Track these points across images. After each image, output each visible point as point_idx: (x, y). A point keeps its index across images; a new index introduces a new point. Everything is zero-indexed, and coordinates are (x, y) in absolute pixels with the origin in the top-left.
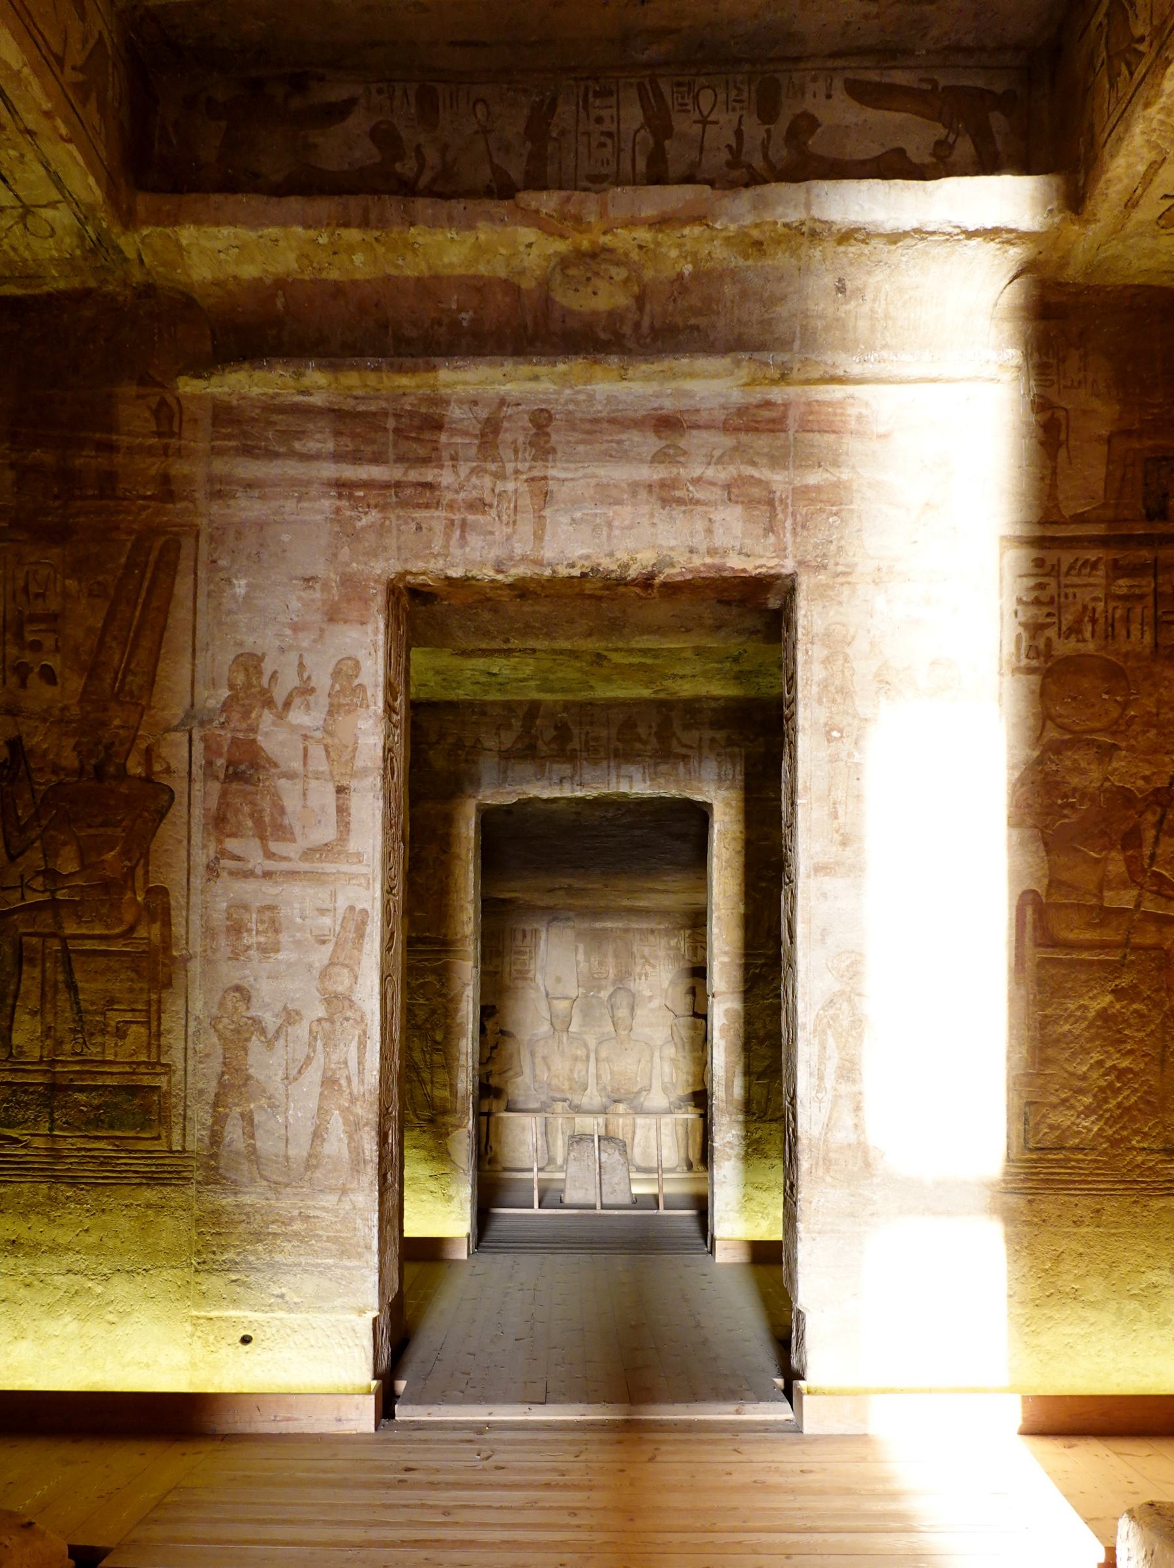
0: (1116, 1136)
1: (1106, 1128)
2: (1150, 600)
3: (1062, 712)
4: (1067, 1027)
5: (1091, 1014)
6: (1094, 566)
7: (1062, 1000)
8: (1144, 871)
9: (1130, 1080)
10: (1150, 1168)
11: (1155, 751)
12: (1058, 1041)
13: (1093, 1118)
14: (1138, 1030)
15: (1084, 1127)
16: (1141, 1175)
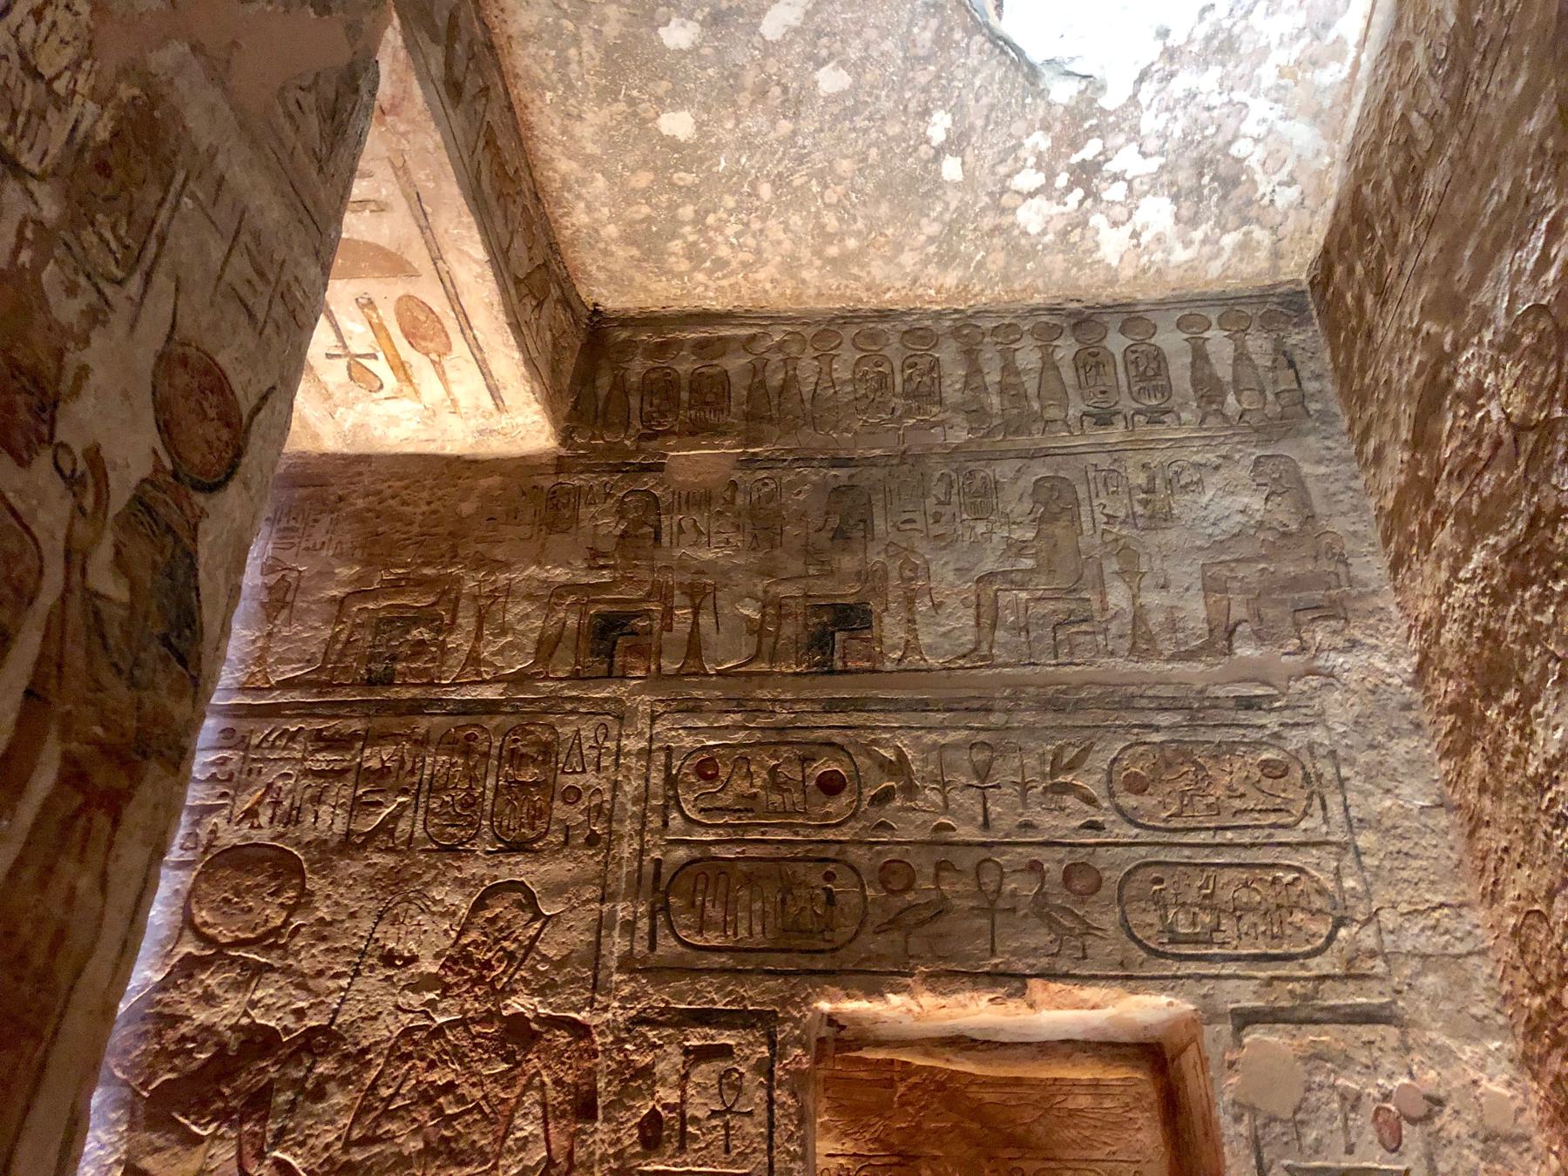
2: (351, 776)
3: (210, 920)
6: (293, 737)
8: (260, 1155)
11: (320, 973)
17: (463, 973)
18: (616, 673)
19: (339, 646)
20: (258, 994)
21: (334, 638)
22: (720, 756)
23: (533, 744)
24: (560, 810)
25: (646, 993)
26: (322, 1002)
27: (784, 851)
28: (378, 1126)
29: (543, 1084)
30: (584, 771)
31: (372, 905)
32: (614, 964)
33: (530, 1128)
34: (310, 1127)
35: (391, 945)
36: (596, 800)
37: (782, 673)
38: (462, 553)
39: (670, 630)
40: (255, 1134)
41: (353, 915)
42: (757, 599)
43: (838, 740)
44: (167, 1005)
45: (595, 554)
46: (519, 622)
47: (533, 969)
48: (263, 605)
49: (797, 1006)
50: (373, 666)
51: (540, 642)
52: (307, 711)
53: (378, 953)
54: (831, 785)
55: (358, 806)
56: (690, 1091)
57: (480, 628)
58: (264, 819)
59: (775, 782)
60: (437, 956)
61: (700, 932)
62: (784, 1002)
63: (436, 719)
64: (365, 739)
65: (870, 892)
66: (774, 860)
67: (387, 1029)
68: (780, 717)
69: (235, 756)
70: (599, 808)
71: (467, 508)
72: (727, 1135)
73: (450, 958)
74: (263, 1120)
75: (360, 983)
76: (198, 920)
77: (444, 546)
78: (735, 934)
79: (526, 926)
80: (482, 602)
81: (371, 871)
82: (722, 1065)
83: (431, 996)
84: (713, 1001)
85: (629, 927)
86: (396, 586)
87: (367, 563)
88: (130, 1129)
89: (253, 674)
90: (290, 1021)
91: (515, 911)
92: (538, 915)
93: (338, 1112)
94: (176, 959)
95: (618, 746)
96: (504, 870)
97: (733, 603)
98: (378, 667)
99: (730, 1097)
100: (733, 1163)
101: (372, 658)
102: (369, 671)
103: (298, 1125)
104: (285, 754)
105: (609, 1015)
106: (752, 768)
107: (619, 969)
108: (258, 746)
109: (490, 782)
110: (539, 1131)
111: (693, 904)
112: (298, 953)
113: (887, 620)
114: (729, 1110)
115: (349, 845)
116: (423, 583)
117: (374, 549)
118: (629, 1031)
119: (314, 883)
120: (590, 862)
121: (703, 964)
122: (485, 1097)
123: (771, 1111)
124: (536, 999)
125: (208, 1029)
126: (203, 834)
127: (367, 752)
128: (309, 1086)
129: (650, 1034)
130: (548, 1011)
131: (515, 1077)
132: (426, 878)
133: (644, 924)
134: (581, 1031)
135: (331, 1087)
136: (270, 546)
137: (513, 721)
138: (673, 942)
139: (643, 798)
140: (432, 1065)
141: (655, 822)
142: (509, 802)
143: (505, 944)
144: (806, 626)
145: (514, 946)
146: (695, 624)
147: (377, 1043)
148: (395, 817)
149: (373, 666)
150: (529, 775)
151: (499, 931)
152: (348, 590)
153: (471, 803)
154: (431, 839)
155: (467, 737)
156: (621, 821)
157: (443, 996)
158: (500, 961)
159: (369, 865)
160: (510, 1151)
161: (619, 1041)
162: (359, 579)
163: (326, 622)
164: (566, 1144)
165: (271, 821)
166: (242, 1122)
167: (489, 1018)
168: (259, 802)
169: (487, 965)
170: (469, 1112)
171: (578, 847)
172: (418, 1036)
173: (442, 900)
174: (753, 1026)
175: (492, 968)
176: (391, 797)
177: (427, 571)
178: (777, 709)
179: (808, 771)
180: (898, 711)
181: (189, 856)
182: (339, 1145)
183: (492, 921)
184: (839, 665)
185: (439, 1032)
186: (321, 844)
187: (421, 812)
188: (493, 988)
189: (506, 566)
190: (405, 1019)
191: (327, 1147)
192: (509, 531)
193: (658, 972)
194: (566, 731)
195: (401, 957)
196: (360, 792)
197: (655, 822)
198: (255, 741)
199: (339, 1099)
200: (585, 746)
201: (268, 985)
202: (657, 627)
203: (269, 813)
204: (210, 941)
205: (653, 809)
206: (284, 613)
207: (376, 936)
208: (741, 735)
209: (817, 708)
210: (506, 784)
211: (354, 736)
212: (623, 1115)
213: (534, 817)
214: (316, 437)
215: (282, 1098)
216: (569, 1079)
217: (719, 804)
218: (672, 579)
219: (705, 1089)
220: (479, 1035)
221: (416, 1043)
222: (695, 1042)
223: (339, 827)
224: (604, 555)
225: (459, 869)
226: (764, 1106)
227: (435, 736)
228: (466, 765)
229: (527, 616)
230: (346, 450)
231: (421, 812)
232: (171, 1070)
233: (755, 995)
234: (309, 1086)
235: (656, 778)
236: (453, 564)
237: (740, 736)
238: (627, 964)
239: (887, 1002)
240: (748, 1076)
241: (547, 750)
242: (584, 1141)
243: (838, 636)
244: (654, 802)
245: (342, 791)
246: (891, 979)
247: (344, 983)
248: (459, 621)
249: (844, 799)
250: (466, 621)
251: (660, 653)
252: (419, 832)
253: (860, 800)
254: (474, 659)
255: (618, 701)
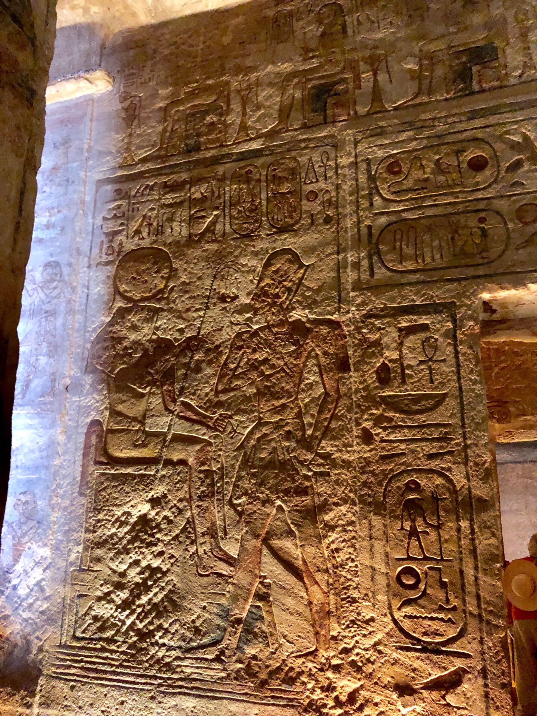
0: (145, 630)
1: (138, 622)
2: (186, 204)
4: (113, 530)
5: (132, 520)
7: (111, 508)
8: (174, 401)
9: (159, 578)
10: (168, 664)
11: (188, 310)
12: (106, 541)
13: (128, 612)
14: (166, 535)
15: (120, 620)
16: (160, 670)
17: (264, 301)
18: (328, 120)
19: (168, 134)
20: (159, 323)
21: (165, 130)
22: (402, 159)
23: (284, 170)
24: (306, 205)
25: (371, 300)
26: (192, 324)
27: (450, 209)
28: (231, 382)
29: (317, 355)
30: (317, 181)
31: (209, 271)
32: (349, 287)
33: (313, 378)
34: (196, 385)
35: (223, 291)
36: (327, 197)
37: (437, 101)
38: (227, 66)
39: (360, 88)
40: (170, 391)
41: (200, 278)
42: (415, 56)
43: (480, 136)
44: (114, 333)
45: (307, 50)
46: (266, 100)
47: (303, 295)
48: (124, 119)
49: (468, 297)
50: (188, 142)
51: (280, 110)
52: (157, 173)
53: (217, 296)
54: (478, 165)
55: (193, 220)
56: (405, 351)
57: (244, 109)
58: (145, 234)
59: (439, 168)
60: (249, 294)
61: (401, 263)
62: (459, 296)
63: (228, 166)
64: (190, 183)
65: (510, 226)
66: (444, 215)
67: (228, 334)
68: (439, 128)
69: (123, 203)
70: (329, 201)
71: (227, 40)
72: (431, 373)
73: (256, 294)
74: (172, 384)
75: (210, 313)
76: (121, 290)
77: (217, 65)
78: (424, 261)
79: (295, 273)
80: (243, 93)
81: (205, 254)
82: (423, 335)
83: (248, 315)
84: (413, 300)
85: (356, 266)
86: (192, 95)
87: (175, 84)
88: (109, 392)
89: (125, 158)
90: (177, 335)
91: (288, 265)
92: (301, 266)
93: (209, 377)
94: (114, 310)
95: (336, 163)
96: (279, 243)
97: (399, 62)
98: (191, 142)
99: (430, 352)
100: (436, 388)
101: (187, 137)
102: (186, 145)
103: (190, 385)
104: (149, 198)
105: (350, 315)
106: (424, 162)
107: (353, 290)
108: (135, 196)
109: (263, 196)
110: (318, 379)
111: (395, 248)
112: (174, 301)
113: (509, 51)
114: (430, 360)
115: (192, 241)
116: (208, 89)
117: (178, 76)
118: (363, 322)
119: (177, 264)
120: (329, 232)
121: (404, 281)
122: (286, 364)
123: (457, 358)
124: (307, 311)
125: (137, 343)
126: (115, 245)
127: (193, 190)
128: (192, 366)
129: (376, 323)
130: (314, 316)
131: (301, 353)
132: (236, 253)
133: (365, 263)
134: (335, 325)
135: (204, 365)
136: (122, 86)
137: (270, 159)
138: (384, 270)
139: (356, 190)
140: (254, 351)
141: (365, 204)
142: (277, 205)
143: (285, 283)
144: (451, 67)
145: (290, 284)
146: (376, 81)
147: (223, 342)
148: (214, 223)
149: (188, 142)
150: (285, 188)
151: (280, 277)
152: (167, 102)
153: (255, 209)
154: (235, 232)
155: (247, 173)
156: (344, 207)
157: (255, 314)
158: (284, 293)
159: (203, 251)
160: (303, 390)
161: (358, 329)
162: (173, 94)
163: (159, 122)
164: (334, 385)
165: (149, 234)
166: (162, 385)
167: (282, 323)
168: (141, 225)
169: (277, 296)
170: (278, 372)
171: (320, 225)
172: (245, 336)
173: (247, 264)
174: (441, 312)
175: (280, 297)
176: (209, 212)
177: (210, 82)
178: (437, 124)
179: (461, 159)
180: (522, 109)
181: (111, 258)
182: (213, 393)
183: (276, 272)
184: (476, 88)
185: (255, 333)
186: (177, 243)
187: (227, 218)
188: (282, 307)
189: (254, 69)
190: (237, 328)
191: (207, 394)
192: (253, 48)
193: (377, 288)
194: (303, 160)
195: (229, 297)
196: (192, 212)
197: (365, 204)
198: (133, 193)
199: (209, 371)
200: (316, 166)
201: (163, 318)
202: (351, 86)
203: (147, 230)
204: (129, 299)
205: (363, 197)
206: (136, 122)
207: (214, 287)
208: (414, 143)
209: (463, 118)
210: (273, 195)
211: (184, 182)
212: (366, 367)
213: (291, 212)
214: (134, 15)
215: (180, 372)
216: (331, 351)
217: (404, 187)
218: (356, 56)
219: (414, 349)
220: (278, 333)
221: (244, 341)
222: (404, 324)
223: (185, 232)
224: (312, 50)
225: (254, 246)
226: (453, 355)
227: (228, 175)
228: (248, 189)
229: (271, 96)
230: (153, 21)
231: (227, 218)
232: (123, 364)
233: (440, 294)
234: (192, 366)
235: (363, 178)
236: (222, 75)
237: (413, 145)
238: (357, 286)
239: (528, 289)
240: (441, 340)
241: (293, 172)
242: (344, 383)
243: (474, 69)
244: (363, 193)
245: (183, 213)
246: (529, 275)
247: (201, 313)
248: (232, 106)
249: (487, 172)
250: (236, 106)
251: (355, 103)
252: (228, 229)
253: (499, 171)
254: (244, 127)
255: (332, 136)
